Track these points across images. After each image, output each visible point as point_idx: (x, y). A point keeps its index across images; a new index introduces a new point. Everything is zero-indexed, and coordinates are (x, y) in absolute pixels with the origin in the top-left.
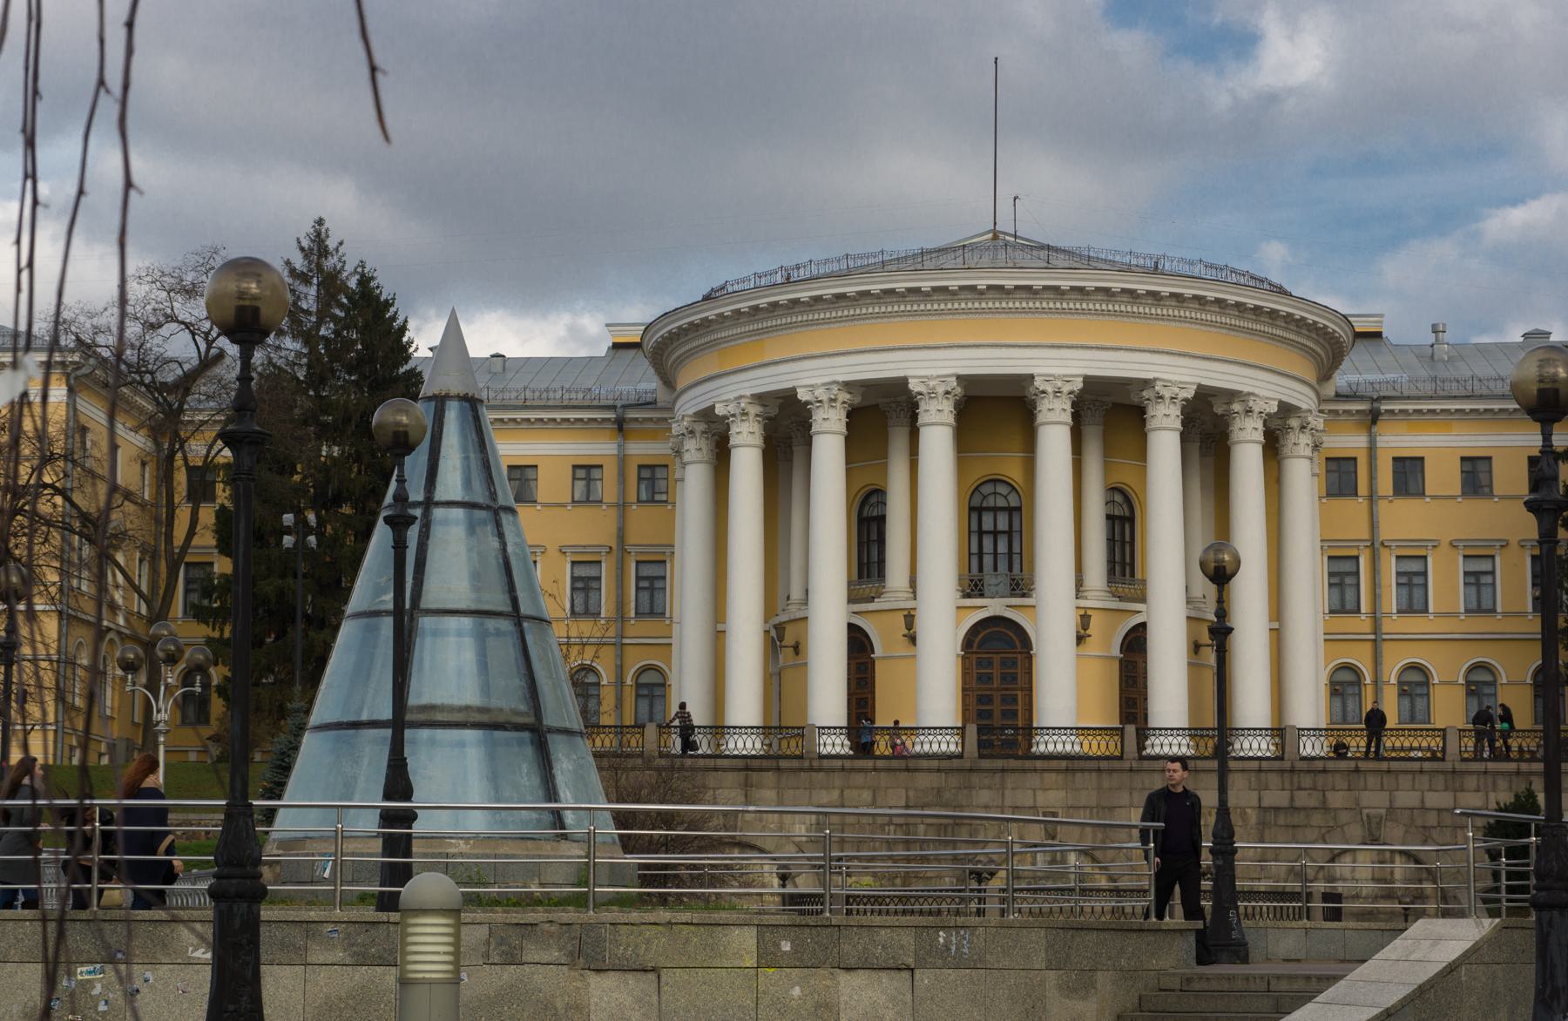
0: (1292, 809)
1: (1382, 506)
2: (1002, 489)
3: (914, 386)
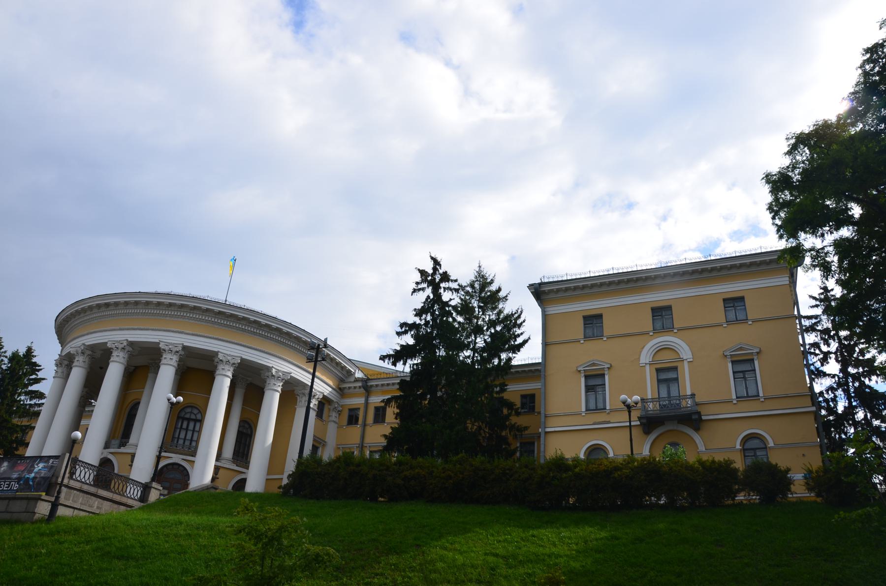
1: (368, 429)
2: (195, 411)
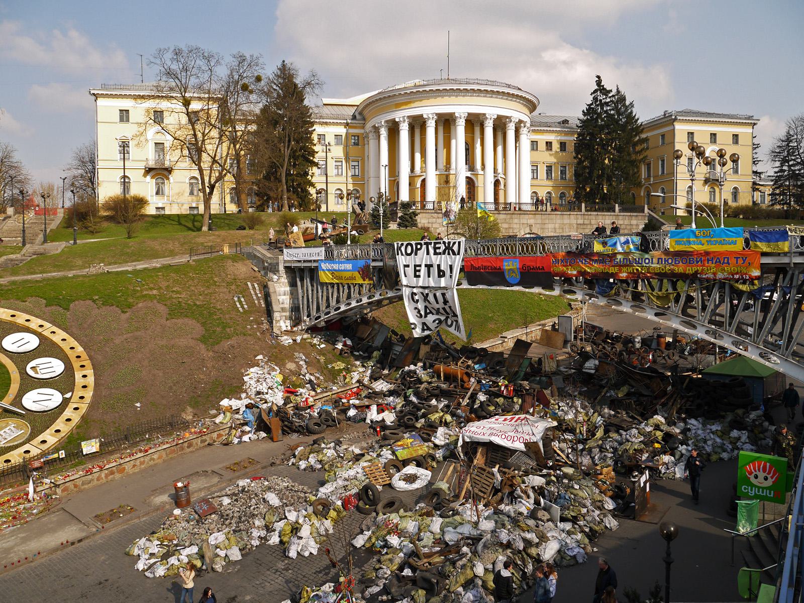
0: (584, 224)
3: (457, 115)
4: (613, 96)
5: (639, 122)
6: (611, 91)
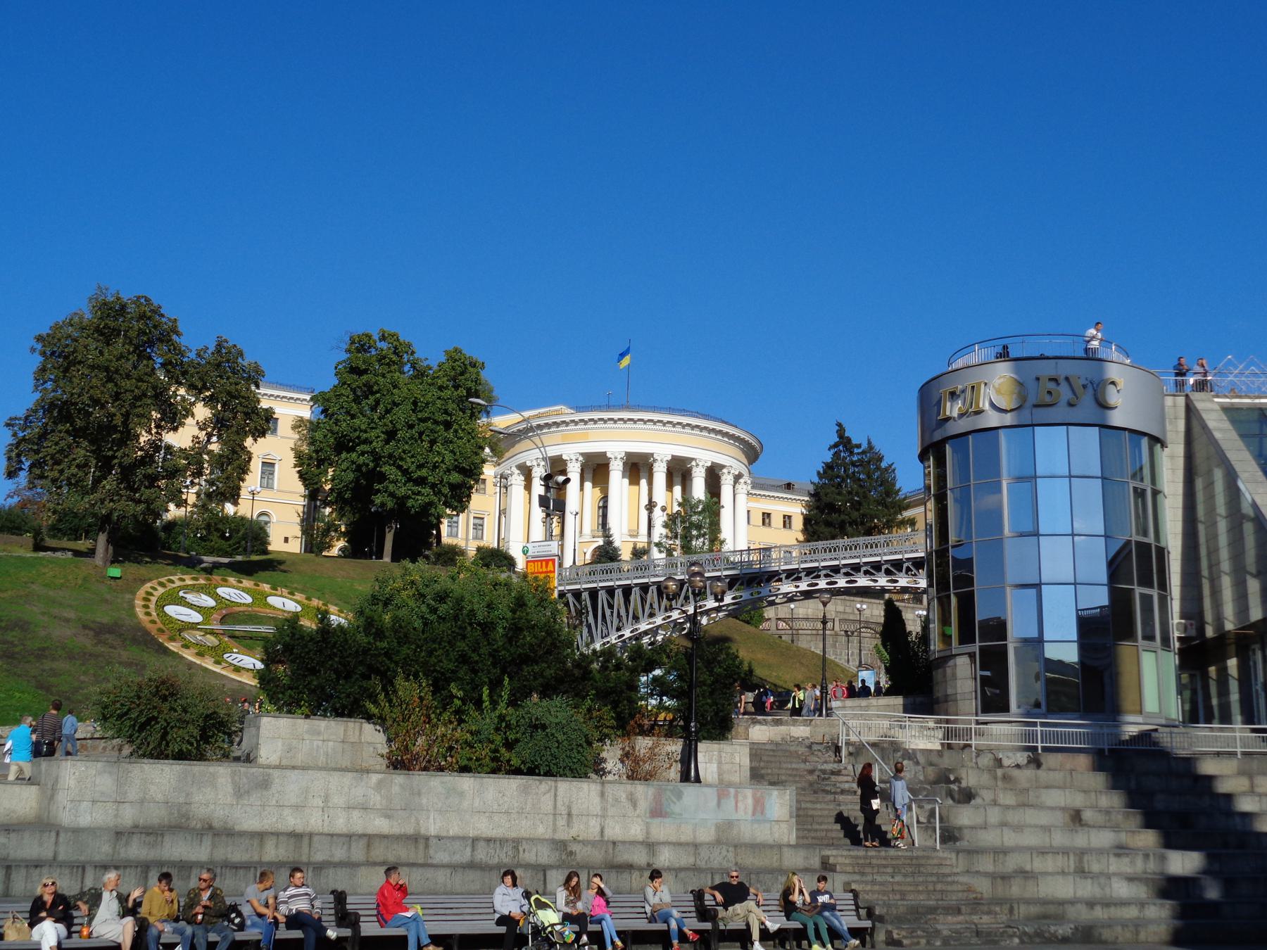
4: (864, 452)
5: (901, 495)
6: (859, 446)
